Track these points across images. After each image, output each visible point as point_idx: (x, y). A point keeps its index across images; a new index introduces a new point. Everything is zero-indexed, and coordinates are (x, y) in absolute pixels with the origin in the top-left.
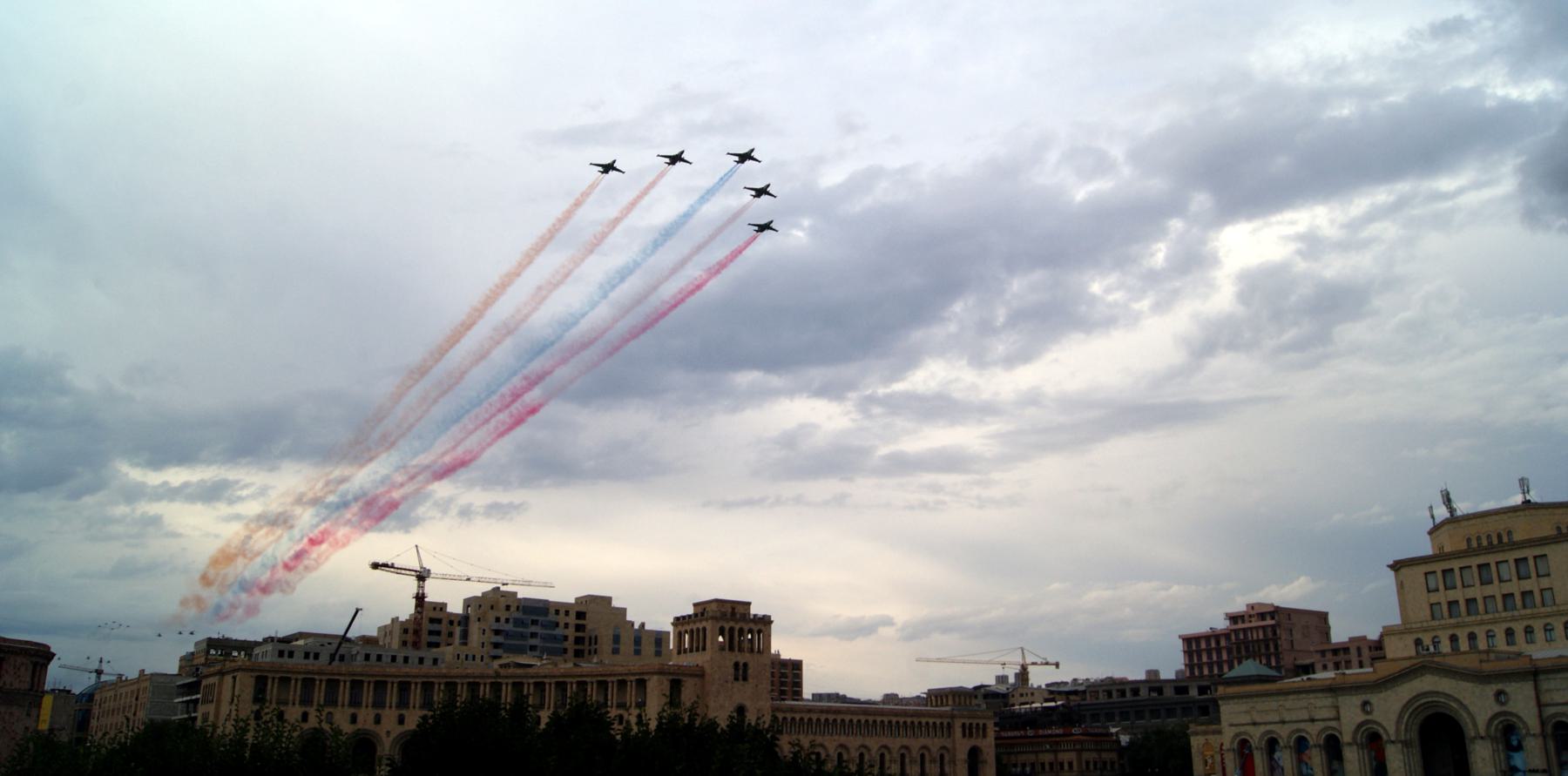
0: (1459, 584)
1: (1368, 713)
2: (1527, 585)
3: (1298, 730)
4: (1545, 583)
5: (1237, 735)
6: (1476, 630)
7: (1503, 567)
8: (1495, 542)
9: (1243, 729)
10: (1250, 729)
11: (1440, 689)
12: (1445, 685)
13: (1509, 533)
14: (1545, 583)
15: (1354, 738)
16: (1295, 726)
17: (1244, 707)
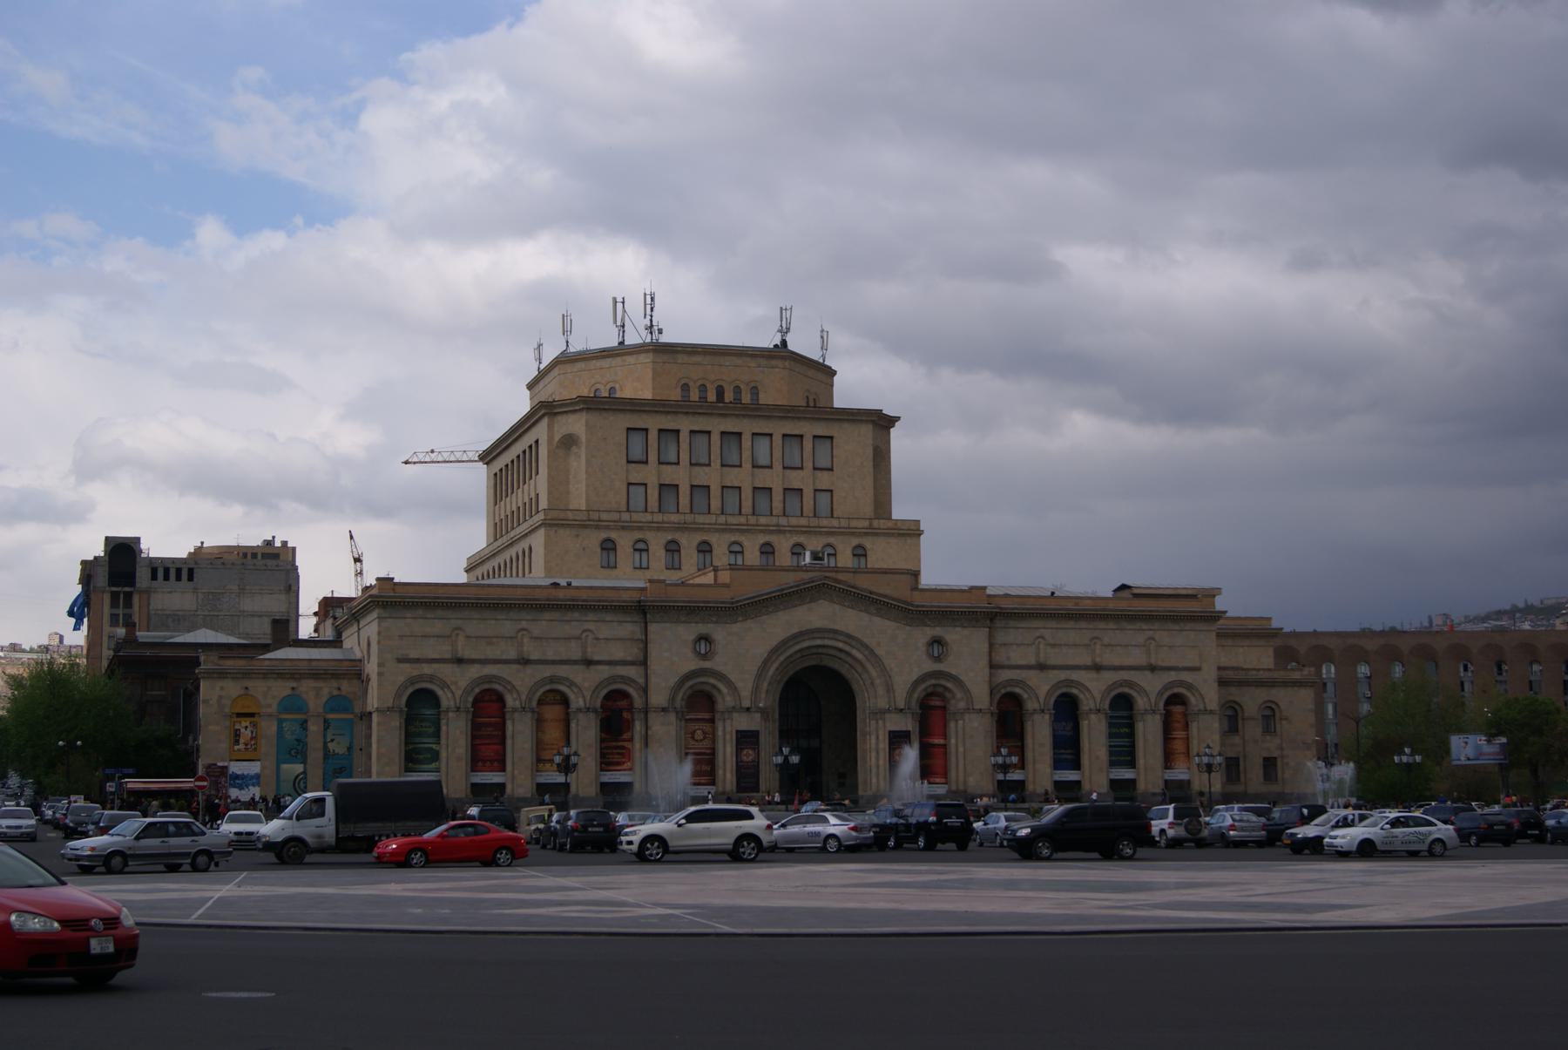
0: (685, 457)
1: (704, 657)
2: (795, 479)
3: (552, 679)
4: (824, 480)
5: (412, 681)
6: (713, 539)
7: (763, 444)
8: (712, 397)
9: (427, 669)
10: (446, 671)
11: (836, 627)
12: (850, 620)
13: (755, 391)
14: (824, 480)
15: (672, 699)
16: (548, 671)
17: (438, 627)
